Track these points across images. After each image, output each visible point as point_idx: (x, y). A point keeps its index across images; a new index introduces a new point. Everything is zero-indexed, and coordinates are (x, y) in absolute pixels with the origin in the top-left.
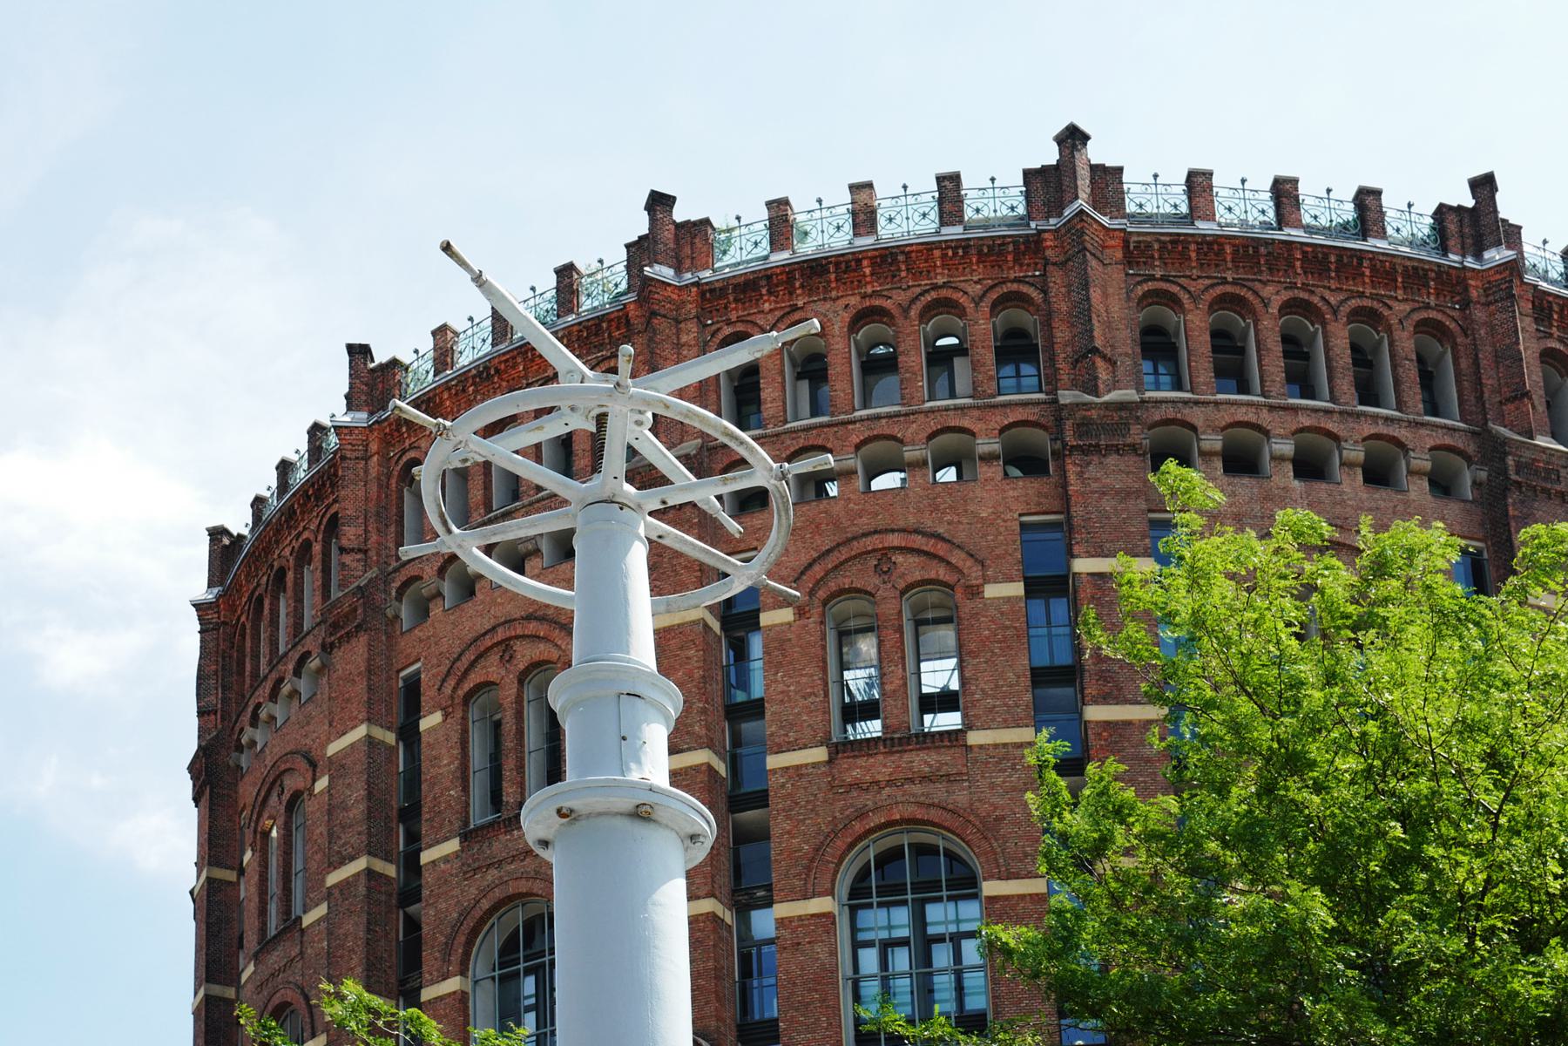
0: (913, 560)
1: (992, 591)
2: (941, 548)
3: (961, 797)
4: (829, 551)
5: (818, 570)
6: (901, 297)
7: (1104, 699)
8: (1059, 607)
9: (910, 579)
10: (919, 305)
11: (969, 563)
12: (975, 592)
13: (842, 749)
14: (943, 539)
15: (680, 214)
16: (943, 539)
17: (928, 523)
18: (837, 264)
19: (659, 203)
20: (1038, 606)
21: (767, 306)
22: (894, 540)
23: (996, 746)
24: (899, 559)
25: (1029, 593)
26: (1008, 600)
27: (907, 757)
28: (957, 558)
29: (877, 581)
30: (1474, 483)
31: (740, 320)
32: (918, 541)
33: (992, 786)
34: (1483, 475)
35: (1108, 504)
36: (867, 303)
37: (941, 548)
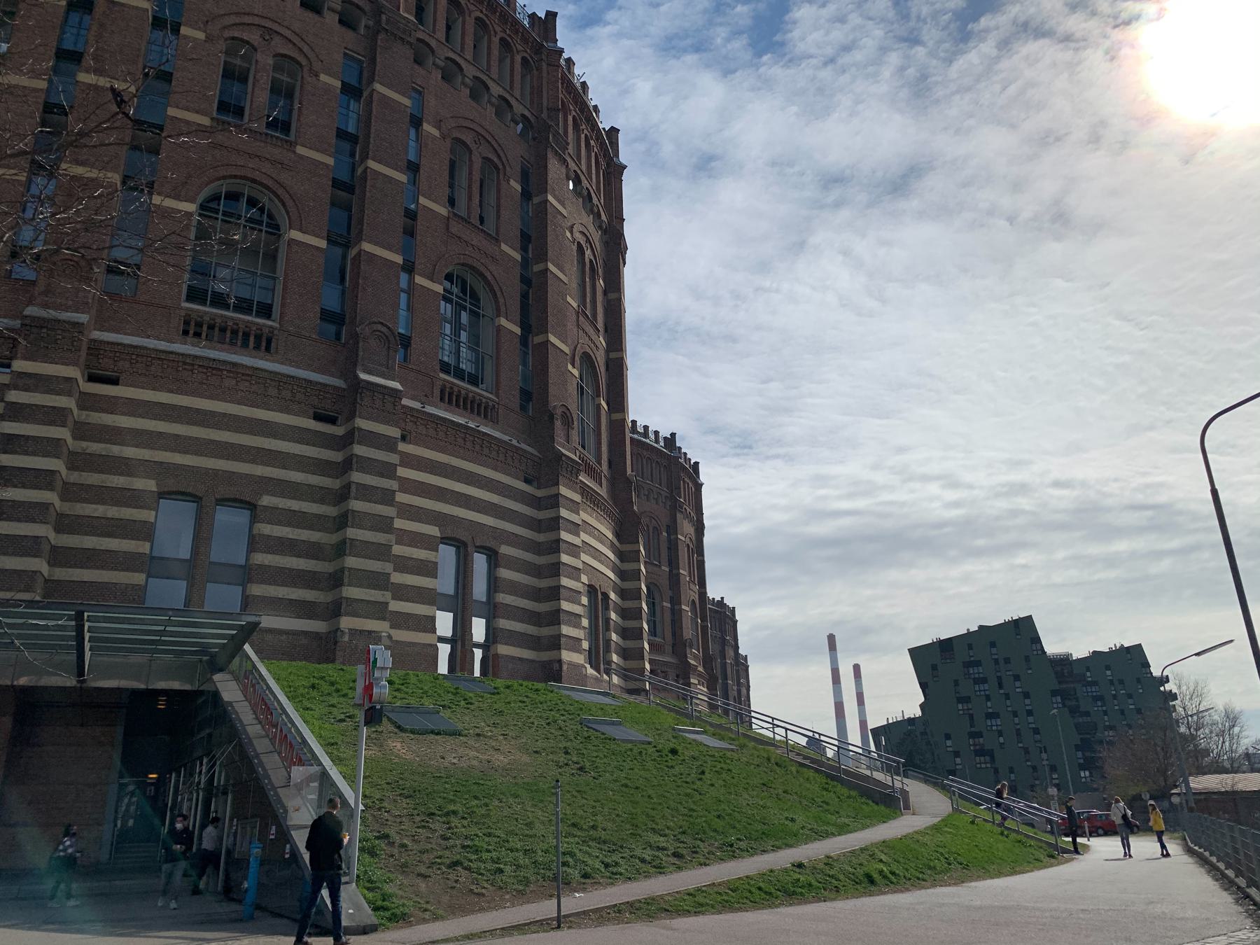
30: (365, 26)
34: (371, 23)
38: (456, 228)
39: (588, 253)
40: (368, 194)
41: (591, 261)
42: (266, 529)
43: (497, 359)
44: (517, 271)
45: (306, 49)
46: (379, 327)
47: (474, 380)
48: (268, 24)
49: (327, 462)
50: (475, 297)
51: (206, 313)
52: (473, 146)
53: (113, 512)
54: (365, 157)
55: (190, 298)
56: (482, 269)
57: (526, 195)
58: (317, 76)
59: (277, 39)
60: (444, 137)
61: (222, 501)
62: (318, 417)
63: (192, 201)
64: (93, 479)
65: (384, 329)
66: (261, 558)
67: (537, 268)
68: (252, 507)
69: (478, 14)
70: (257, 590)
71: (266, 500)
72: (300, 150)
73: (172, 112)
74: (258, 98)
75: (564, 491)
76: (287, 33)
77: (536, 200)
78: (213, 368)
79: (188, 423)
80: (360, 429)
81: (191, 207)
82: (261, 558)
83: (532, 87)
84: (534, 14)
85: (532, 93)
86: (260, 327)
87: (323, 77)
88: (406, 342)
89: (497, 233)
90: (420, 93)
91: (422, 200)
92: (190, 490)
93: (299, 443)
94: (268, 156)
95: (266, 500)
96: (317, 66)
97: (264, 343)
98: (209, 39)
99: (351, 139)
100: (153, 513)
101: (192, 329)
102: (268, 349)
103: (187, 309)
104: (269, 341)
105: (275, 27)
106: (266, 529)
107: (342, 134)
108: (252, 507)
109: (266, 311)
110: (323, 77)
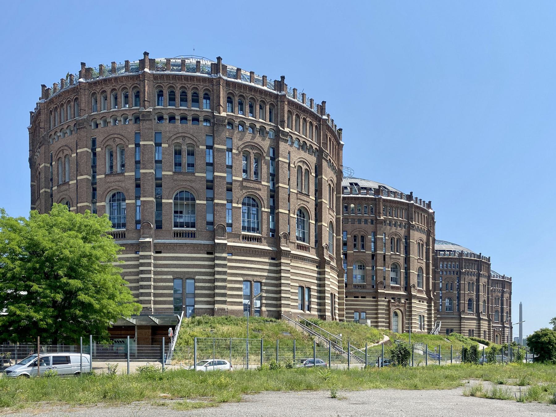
0: (118, 139)
1: (130, 146)
2: (122, 138)
3: (123, 185)
4: (106, 137)
5: (104, 141)
6: (118, 87)
7: (143, 168)
9: (118, 143)
10: (121, 89)
11: (126, 141)
12: (127, 146)
14: (123, 136)
15: (87, 67)
16: (123, 136)
17: (121, 132)
18: (108, 80)
19: (83, 64)
21: (98, 87)
22: (116, 136)
23: (129, 175)
24: (116, 139)
26: (132, 148)
27: (116, 177)
28: (125, 140)
29: (113, 143)
31: (94, 90)
32: (119, 136)
33: (128, 183)
35: (146, 131)
36: (113, 88)
37: (122, 138)
40: (215, 184)
42: (197, 284)
43: (262, 222)
45: (195, 139)
46: (221, 225)
48: (184, 135)
49: (211, 265)
51: (178, 230)
53: (164, 284)
55: (175, 226)
58: (199, 147)
59: (187, 139)
61: (187, 279)
62: (208, 253)
63: (171, 199)
64: (159, 277)
65: (222, 226)
66: (197, 292)
68: (194, 279)
69: (251, 96)
70: (197, 299)
71: (197, 277)
72: (197, 174)
73: (164, 173)
74: (185, 159)
76: (189, 136)
78: (181, 245)
79: (177, 261)
80: (216, 256)
81: (171, 201)
82: (197, 292)
85: (275, 117)
86: (191, 231)
87: (201, 147)
88: (230, 225)
90: (232, 138)
92: (180, 277)
93: (203, 261)
94: (188, 179)
95: (197, 277)
96: (198, 143)
97: (192, 235)
98: (169, 146)
99: (211, 165)
100: (173, 283)
101: (177, 235)
102: (194, 237)
103: (174, 230)
104: (194, 234)
105: (185, 135)
106: (197, 284)
107: (208, 164)
108: (194, 279)
110: (201, 147)
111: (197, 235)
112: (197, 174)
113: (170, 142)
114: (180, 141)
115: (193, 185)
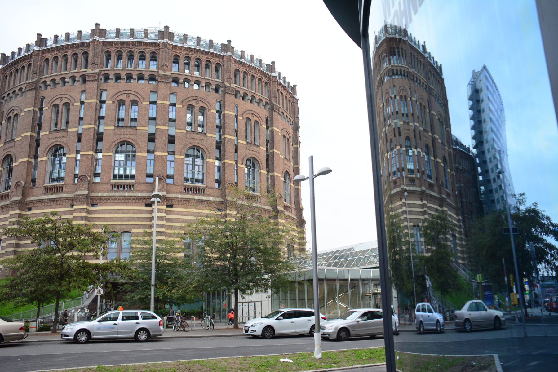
8: (155, 106)
13: (118, 127)
20: (151, 105)
25: (150, 104)
32: (133, 93)
38: (248, 146)
39: (287, 136)
41: (288, 139)
44: (265, 154)
47: (254, 190)
50: (253, 164)
52: (251, 118)
54: (224, 133)
56: (255, 157)
57: (267, 128)
60: (243, 119)
67: (270, 151)
75: (280, 220)
77: (270, 129)
83: (268, 90)
84: (268, 64)
89: (259, 144)
91: (239, 141)
109: (202, 181)
110: (212, 111)
111: (207, 191)
112: (208, 135)
113: (184, 104)
114: (193, 103)
115: (205, 143)
